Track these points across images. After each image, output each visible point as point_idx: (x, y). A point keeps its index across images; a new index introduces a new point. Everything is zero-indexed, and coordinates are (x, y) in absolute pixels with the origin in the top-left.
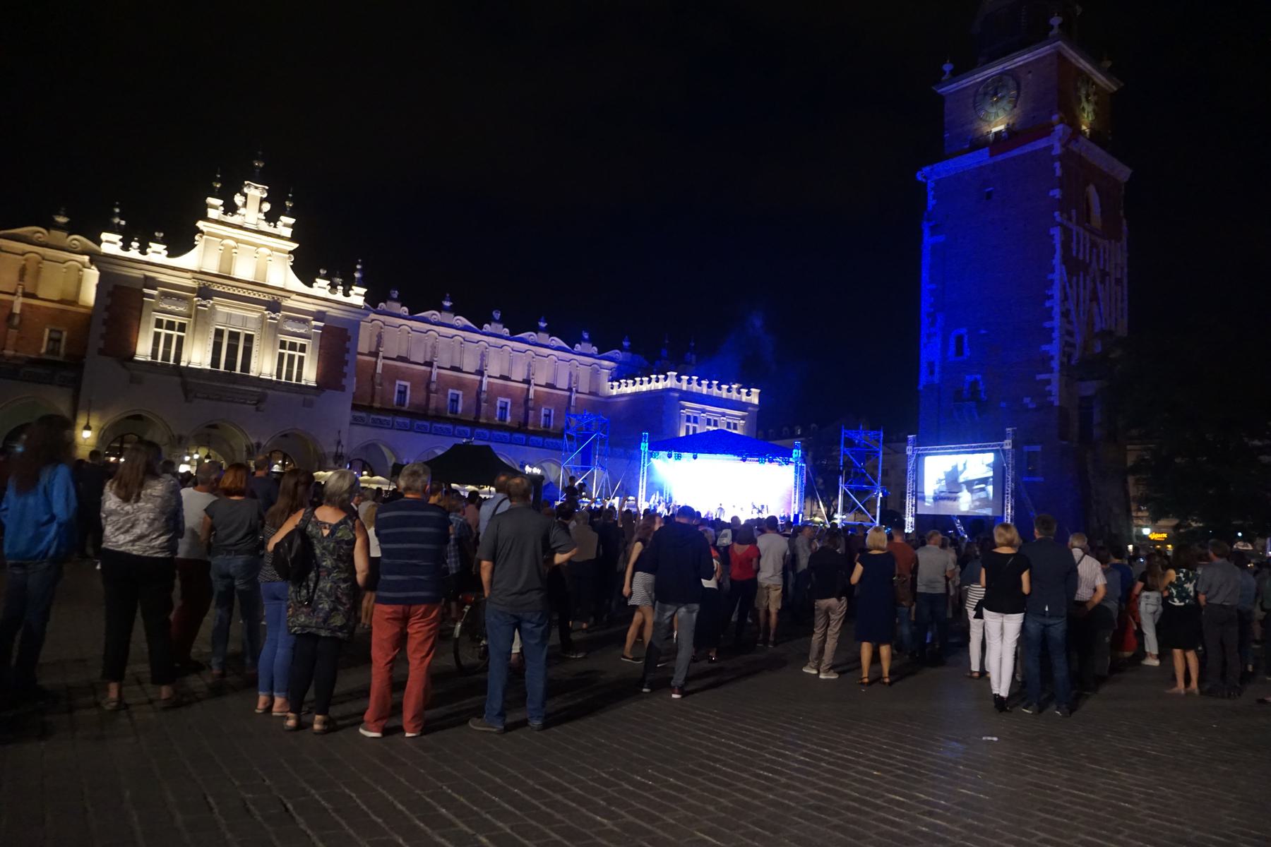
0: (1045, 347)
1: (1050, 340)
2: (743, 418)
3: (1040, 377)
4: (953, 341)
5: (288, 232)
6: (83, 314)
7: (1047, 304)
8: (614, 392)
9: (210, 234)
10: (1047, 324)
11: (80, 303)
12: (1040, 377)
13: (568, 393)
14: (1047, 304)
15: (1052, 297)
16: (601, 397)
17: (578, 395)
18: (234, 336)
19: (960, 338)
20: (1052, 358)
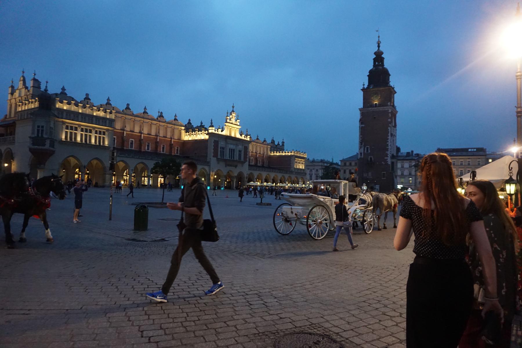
0: (387, 152)
1: (388, 151)
2: (304, 161)
3: (385, 158)
4: (366, 148)
5: (238, 124)
6: (181, 142)
7: (387, 143)
8: (272, 154)
9: (228, 126)
10: (387, 147)
11: (181, 139)
12: (385, 158)
13: (170, 139)
14: (387, 143)
15: (388, 142)
16: (182, 140)
17: (174, 140)
18: (232, 149)
19: (368, 148)
20: (388, 154)
